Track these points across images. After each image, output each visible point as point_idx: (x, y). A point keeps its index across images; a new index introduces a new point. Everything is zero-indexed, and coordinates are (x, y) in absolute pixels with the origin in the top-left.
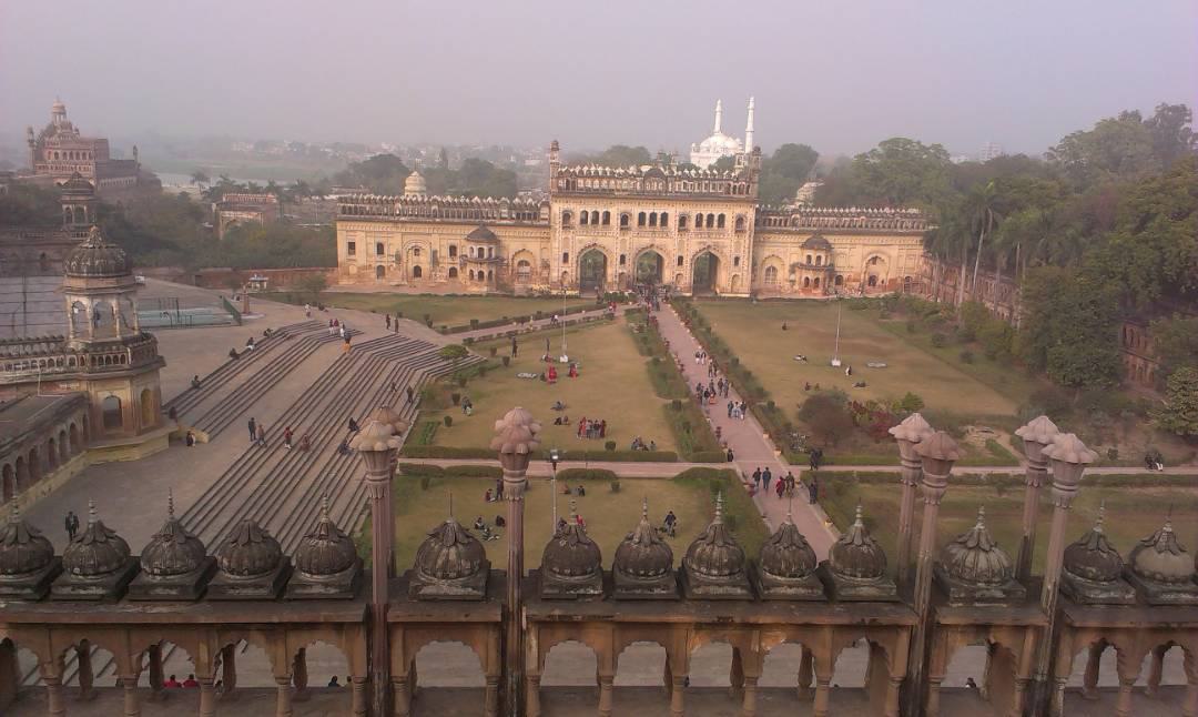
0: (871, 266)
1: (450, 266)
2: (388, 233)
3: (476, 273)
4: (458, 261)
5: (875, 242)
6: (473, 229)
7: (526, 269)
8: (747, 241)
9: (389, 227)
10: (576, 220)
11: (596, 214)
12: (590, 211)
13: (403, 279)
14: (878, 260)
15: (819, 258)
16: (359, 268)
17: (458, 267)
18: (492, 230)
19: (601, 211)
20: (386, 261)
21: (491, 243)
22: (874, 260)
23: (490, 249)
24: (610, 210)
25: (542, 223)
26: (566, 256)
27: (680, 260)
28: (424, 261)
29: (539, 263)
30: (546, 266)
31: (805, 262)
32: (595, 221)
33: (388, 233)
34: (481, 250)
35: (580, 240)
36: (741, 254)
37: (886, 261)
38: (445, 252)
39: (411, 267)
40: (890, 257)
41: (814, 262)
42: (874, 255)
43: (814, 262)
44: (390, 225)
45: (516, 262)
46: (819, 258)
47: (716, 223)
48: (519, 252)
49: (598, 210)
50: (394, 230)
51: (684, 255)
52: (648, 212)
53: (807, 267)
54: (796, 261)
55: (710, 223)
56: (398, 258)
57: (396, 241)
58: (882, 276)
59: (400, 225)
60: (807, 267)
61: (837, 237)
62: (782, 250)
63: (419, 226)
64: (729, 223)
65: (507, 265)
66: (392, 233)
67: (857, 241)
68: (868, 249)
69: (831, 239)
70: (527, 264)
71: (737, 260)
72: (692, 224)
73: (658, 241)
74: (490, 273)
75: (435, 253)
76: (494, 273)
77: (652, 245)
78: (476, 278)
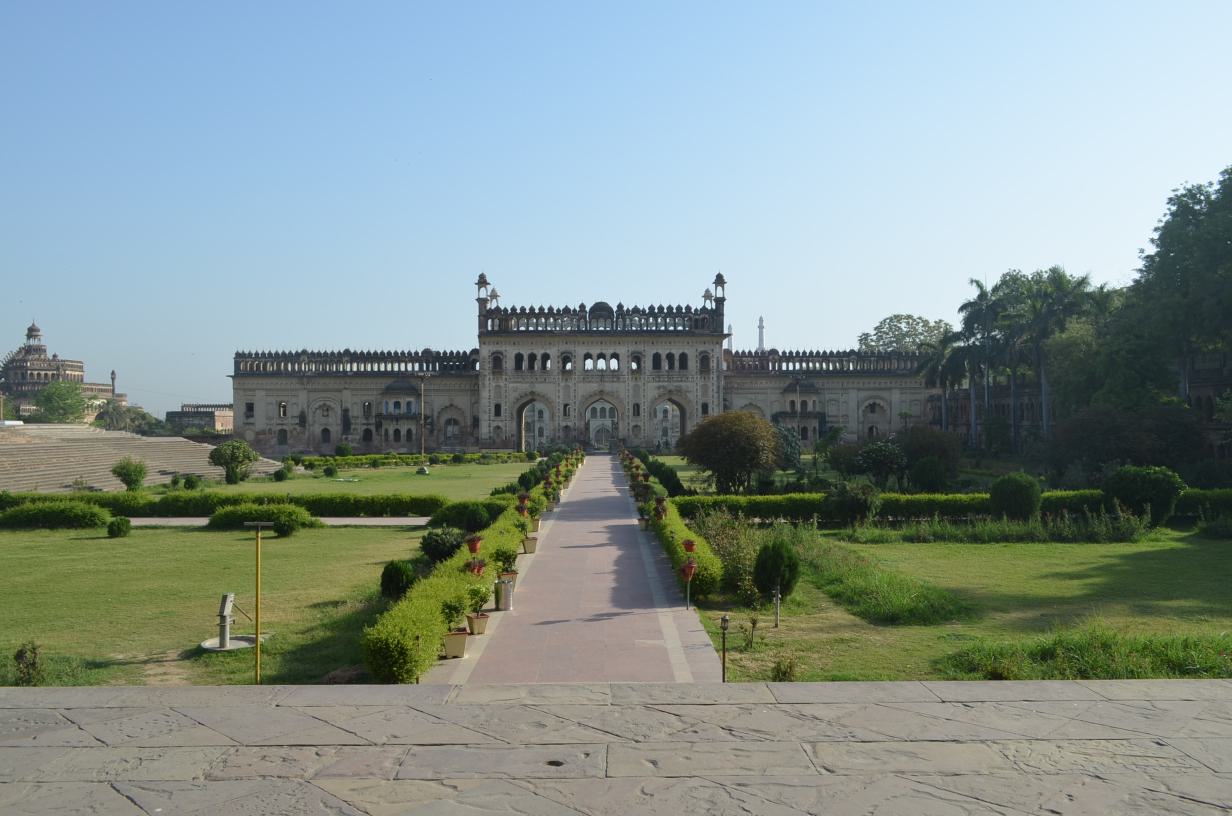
0: (870, 415)
1: (365, 427)
2: (292, 390)
3: (391, 432)
4: (373, 421)
5: (872, 385)
6: (389, 381)
7: (456, 428)
8: (715, 383)
9: (293, 383)
10: (509, 364)
11: (532, 357)
12: (526, 353)
13: (308, 444)
14: (877, 409)
15: (804, 404)
16: (258, 433)
17: (373, 428)
18: (414, 382)
19: (539, 353)
20: (290, 424)
21: (408, 395)
22: (873, 408)
23: (409, 404)
24: (548, 352)
25: (472, 373)
26: (498, 408)
27: (637, 407)
28: (335, 425)
29: (469, 422)
30: (476, 422)
31: (788, 409)
32: (531, 367)
33: (292, 390)
34: (397, 405)
35: (512, 388)
36: (709, 401)
37: (886, 407)
38: (356, 411)
39: (318, 430)
40: (890, 404)
41: (798, 407)
42: (871, 401)
43: (798, 407)
44: (294, 381)
45: (443, 420)
46: (804, 404)
47: (677, 364)
48: (446, 407)
49: (535, 352)
50: (298, 386)
51: (641, 402)
52: (595, 352)
53: (793, 414)
54: (778, 410)
55: (671, 366)
56: (302, 419)
57: (300, 400)
58: (882, 427)
59: (305, 380)
60: (793, 414)
61: (826, 381)
62: (761, 397)
63: (327, 380)
64: (693, 363)
65: (431, 424)
66: (296, 390)
67: (850, 386)
68: (863, 394)
69: (818, 383)
70: (456, 422)
71: (705, 407)
72: (648, 363)
73: (608, 387)
74: (409, 432)
75: (346, 412)
76: (414, 432)
77: (601, 392)
78: (392, 437)
